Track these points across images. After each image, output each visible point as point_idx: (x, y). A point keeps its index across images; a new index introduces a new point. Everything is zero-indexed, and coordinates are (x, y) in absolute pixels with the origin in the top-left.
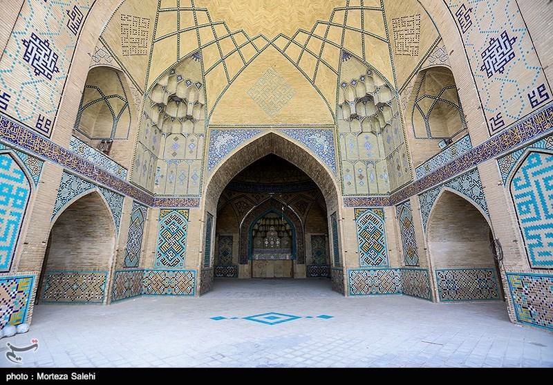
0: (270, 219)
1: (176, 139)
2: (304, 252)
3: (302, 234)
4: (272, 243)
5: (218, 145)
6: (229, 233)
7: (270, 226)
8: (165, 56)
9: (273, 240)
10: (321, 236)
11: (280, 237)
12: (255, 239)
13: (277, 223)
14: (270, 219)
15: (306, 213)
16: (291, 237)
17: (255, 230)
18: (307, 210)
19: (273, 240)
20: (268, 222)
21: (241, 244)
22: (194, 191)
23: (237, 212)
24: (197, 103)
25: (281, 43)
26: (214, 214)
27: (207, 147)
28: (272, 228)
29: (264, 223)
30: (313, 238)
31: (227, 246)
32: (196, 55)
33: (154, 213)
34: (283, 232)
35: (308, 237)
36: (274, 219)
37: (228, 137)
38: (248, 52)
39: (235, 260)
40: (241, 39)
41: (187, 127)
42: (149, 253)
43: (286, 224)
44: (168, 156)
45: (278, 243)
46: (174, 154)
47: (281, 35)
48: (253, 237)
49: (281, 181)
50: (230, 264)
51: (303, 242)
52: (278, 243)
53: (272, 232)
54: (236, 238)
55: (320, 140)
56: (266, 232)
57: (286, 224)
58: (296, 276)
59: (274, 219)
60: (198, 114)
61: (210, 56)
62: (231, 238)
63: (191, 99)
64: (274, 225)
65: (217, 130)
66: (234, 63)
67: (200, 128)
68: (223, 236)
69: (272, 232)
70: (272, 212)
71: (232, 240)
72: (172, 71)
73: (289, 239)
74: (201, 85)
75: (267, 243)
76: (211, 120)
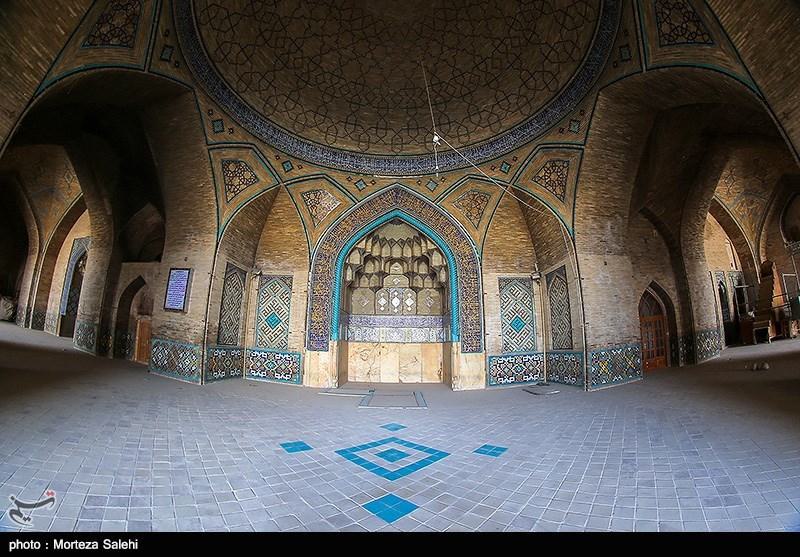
0: (392, 243)
2: (480, 324)
3: (474, 275)
4: (396, 302)
6: (285, 268)
7: (392, 260)
9: (398, 295)
10: (522, 281)
11: (416, 289)
12: (356, 295)
13: (408, 254)
14: (392, 243)
15: (485, 221)
16: (442, 288)
17: (352, 266)
18: (488, 212)
19: (398, 295)
20: (386, 252)
21: (314, 299)
23: (307, 217)
28: (397, 268)
29: (376, 253)
30: (503, 283)
31: (279, 302)
34: (423, 277)
35: (490, 281)
36: (402, 243)
39: (296, 338)
43: (430, 252)
45: (409, 302)
48: (351, 287)
49: (419, 151)
50: (283, 347)
51: (476, 295)
52: (409, 302)
53: (396, 275)
54: (302, 279)
56: (382, 274)
57: (430, 252)
58: (459, 386)
59: (402, 243)
62: (287, 281)
64: (402, 260)
68: (269, 278)
69: (396, 275)
70: (397, 221)
71: (290, 286)
73: (435, 294)
75: (383, 301)
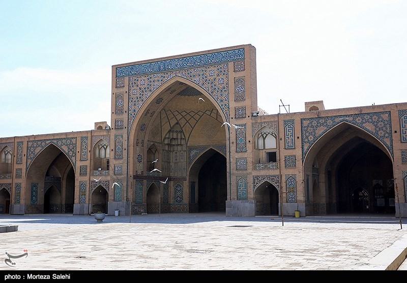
1: (176, 153)
5: (191, 155)
8: (166, 128)
22: (184, 175)
24: (181, 139)
26: (197, 181)
27: (188, 156)
32: (177, 123)
33: (172, 183)
37: (195, 151)
38: (197, 117)
40: (192, 114)
41: (180, 148)
42: (171, 198)
44: (174, 161)
46: (176, 160)
47: (207, 110)
60: (183, 142)
61: (183, 122)
63: (179, 137)
65: (190, 149)
66: (192, 122)
67: (184, 148)
72: (170, 131)
74: (182, 132)
76: (188, 145)
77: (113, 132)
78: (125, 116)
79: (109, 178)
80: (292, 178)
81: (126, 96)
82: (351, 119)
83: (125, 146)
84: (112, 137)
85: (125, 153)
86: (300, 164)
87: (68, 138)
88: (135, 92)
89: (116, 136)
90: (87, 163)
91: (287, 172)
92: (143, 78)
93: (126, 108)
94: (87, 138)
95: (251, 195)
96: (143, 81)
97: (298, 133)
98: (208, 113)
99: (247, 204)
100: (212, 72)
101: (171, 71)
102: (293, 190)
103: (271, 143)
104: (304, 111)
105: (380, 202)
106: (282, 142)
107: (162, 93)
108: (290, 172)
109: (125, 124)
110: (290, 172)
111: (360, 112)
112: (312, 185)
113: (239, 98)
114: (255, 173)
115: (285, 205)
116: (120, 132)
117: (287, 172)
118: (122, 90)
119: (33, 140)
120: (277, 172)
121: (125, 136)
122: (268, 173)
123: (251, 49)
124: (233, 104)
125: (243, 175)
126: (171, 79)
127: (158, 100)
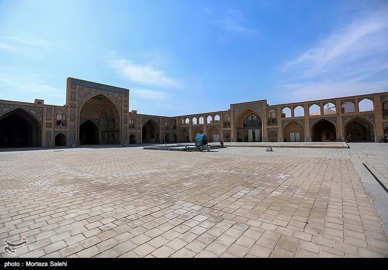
25: (93, 106)
55: (97, 121)
77: (69, 109)
78: (77, 103)
79: (67, 130)
80: (139, 133)
81: (77, 94)
82: (24, 107)
83: (76, 116)
84: (69, 112)
85: (76, 119)
86: (141, 129)
87: (36, 107)
88: (82, 93)
89: (71, 111)
90: (52, 121)
91: (138, 131)
92: (86, 88)
93: (77, 99)
94: (51, 109)
95: (128, 138)
96: (86, 89)
97: (141, 120)
98: (93, 106)
99: (127, 141)
100: (116, 95)
101: (100, 90)
102: (139, 137)
103: (59, 117)
104: (34, 103)
105: (111, 139)
106: (69, 119)
107: (107, 98)
108: (139, 131)
109: (77, 106)
110: (139, 131)
111: (155, 117)
112: (77, 136)
113: (74, 100)
114: (130, 131)
115: (68, 142)
116: (74, 109)
117: (138, 131)
118: (75, 90)
119: (146, 116)
120: (135, 131)
121: (77, 112)
122: (60, 129)
123: (126, 92)
124: (123, 108)
125: (125, 131)
126: (99, 92)
127: (109, 101)
